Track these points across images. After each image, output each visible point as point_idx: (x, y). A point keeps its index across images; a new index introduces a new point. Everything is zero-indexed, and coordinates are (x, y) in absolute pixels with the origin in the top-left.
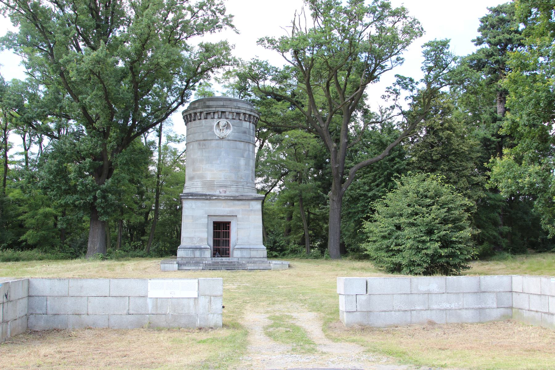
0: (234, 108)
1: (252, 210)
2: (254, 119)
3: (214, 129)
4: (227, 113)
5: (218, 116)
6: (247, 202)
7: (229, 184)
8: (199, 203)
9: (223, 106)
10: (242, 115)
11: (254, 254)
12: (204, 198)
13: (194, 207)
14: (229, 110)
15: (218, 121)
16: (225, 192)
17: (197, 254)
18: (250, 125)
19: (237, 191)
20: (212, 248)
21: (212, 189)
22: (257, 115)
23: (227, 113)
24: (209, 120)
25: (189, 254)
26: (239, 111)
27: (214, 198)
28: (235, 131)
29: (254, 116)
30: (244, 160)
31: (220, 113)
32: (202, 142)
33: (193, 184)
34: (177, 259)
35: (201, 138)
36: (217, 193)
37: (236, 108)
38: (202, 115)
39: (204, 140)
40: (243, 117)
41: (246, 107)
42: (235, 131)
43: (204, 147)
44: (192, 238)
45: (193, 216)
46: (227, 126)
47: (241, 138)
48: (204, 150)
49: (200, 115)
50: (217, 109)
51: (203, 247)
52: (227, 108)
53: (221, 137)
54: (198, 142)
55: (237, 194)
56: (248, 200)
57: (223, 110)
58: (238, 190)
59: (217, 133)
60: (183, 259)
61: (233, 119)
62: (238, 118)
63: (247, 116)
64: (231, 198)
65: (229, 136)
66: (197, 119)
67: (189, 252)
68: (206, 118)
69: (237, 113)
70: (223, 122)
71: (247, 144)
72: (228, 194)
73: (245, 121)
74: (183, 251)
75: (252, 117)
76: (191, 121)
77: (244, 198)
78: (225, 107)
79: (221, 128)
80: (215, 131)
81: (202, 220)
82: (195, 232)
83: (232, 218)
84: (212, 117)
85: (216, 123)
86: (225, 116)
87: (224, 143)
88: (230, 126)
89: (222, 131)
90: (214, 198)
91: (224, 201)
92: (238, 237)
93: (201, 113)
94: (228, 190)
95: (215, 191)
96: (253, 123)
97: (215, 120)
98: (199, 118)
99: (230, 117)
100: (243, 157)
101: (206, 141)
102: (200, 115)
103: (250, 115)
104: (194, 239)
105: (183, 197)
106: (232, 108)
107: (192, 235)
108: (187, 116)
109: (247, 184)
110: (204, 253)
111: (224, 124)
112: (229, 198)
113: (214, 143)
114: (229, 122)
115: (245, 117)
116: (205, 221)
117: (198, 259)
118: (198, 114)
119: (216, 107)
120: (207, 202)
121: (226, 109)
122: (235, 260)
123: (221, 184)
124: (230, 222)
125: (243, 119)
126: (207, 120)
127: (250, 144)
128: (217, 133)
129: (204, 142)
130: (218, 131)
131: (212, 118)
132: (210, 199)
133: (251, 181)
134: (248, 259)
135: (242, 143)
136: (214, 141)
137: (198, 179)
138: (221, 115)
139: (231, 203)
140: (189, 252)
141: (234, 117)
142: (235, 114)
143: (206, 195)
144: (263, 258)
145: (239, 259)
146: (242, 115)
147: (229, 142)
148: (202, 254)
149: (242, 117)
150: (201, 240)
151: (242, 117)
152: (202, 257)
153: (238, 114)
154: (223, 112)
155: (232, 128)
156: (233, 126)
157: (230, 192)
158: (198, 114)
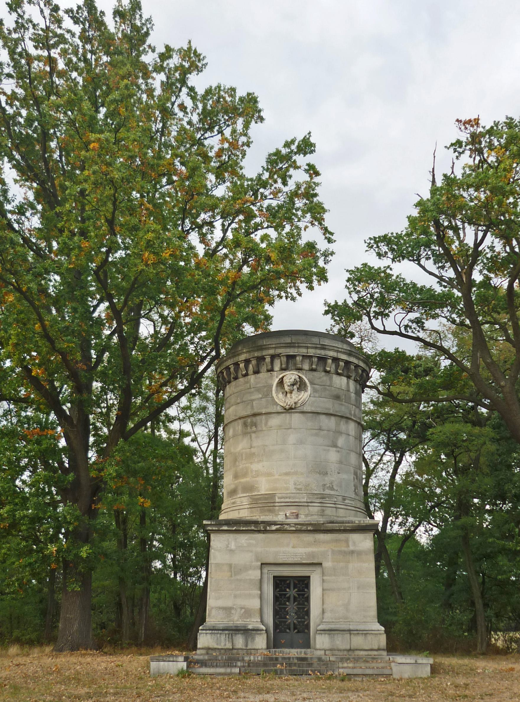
0: (312, 348)
1: (352, 552)
2: (357, 372)
3: (274, 392)
4: (298, 358)
5: (281, 365)
6: (342, 536)
8: (243, 539)
9: (290, 345)
10: (330, 361)
11: (358, 641)
12: (253, 528)
13: (233, 546)
14: (303, 351)
15: (281, 376)
16: (297, 516)
17: (239, 641)
18: (348, 383)
19: (322, 513)
21: (270, 511)
22: (361, 364)
23: (299, 359)
24: (263, 375)
26: (323, 353)
27: (274, 528)
29: (357, 366)
30: (338, 452)
31: (284, 359)
33: (234, 503)
34: (198, 652)
35: (249, 412)
36: (280, 518)
37: (316, 348)
38: (251, 367)
39: (255, 415)
40: (333, 366)
41: (340, 346)
42: (317, 395)
43: (254, 429)
44: (228, 610)
45: (230, 566)
46: (300, 385)
48: (253, 435)
49: (246, 367)
50: (279, 351)
51: (250, 627)
52: (299, 347)
53: (287, 407)
54: (242, 420)
55: (321, 520)
56: (345, 531)
58: (323, 511)
59: (280, 399)
60: (210, 652)
61: (312, 370)
63: (342, 364)
64: (309, 528)
65: (303, 404)
66: (240, 375)
67: (223, 637)
68: (257, 372)
69: (318, 357)
70: (290, 376)
71: (343, 421)
72: (302, 519)
74: (209, 636)
75: (352, 367)
76: (229, 382)
77: (336, 526)
78: (294, 347)
79: (287, 388)
80: (274, 395)
81: (250, 572)
82: (235, 596)
83: (311, 568)
84: (269, 367)
85: (278, 380)
86: (295, 364)
87: (296, 418)
88: (305, 384)
89: (288, 395)
90: (274, 528)
91: (295, 535)
93: (247, 362)
94: (303, 512)
95: (277, 515)
96: (356, 381)
97: (275, 373)
98: (244, 372)
99: (306, 367)
100: (335, 446)
101: (258, 418)
102: (246, 367)
103: (347, 363)
105: (209, 528)
107: (229, 603)
108: (222, 372)
109: (344, 500)
110: (253, 639)
111: (292, 380)
112: (304, 528)
113: (275, 421)
114: (304, 377)
115: (337, 367)
116: (256, 574)
117: (240, 652)
118: (242, 365)
119: (275, 348)
121: (296, 350)
122: (320, 653)
123: (288, 500)
124: (309, 577)
125: (333, 370)
126: (261, 375)
127: (350, 421)
128: (280, 399)
129: (254, 419)
130: (281, 395)
131: (268, 371)
132: (265, 531)
133: (353, 496)
134: (345, 653)
135: (333, 418)
136: (273, 415)
140: (223, 637)
141: (314, 367)
142: (315, 360)
143: (256, 523)
144: (379, 650)
146: (330, 361)
148: (249, 642)
149: (330, 366)
150: (248, 612)
151: (330, 366)
152: (249, 647)
153: (322, 360)
154: (291, 358)
155: (309, 388)
156: (312, 383)
157: (306, 515)
158: (242, 365)
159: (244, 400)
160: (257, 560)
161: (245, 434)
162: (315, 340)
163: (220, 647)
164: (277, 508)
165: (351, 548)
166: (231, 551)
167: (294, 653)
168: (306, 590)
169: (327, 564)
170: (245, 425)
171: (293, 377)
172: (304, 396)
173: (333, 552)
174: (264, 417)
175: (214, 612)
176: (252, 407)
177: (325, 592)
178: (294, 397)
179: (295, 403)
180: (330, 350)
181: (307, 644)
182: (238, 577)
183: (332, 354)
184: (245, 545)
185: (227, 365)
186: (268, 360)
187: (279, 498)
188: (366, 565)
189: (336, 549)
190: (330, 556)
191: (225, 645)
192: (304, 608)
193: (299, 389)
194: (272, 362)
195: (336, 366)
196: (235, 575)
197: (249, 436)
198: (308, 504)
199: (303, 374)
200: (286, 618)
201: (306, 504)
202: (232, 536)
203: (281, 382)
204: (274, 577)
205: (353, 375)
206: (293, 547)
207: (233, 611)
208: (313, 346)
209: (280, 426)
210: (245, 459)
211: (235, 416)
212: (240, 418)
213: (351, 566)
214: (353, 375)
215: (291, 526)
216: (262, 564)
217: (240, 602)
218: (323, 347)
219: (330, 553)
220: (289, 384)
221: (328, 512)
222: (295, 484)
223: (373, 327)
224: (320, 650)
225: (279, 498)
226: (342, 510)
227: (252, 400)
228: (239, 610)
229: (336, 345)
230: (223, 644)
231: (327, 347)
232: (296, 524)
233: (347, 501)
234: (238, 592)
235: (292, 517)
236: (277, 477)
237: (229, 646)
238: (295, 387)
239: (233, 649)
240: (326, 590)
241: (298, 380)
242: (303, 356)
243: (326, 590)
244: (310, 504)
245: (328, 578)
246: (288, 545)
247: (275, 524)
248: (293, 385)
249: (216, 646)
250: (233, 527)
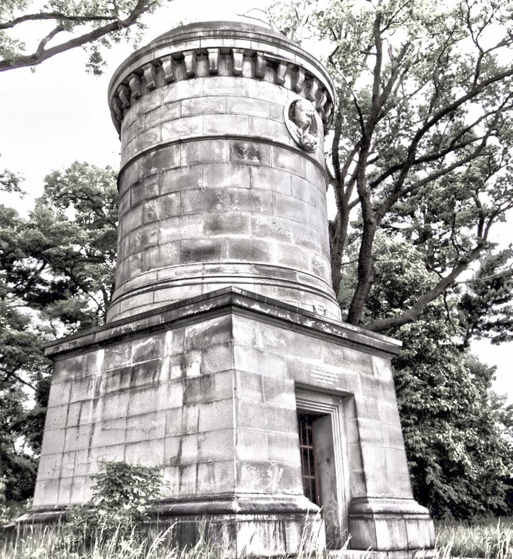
12: (288, 317)
32: (246, 145)
39: (258, 140)
43: (256, 160)
45: (259, 378)
104: (270, 473)
123: (311, 285)
129: (256, 146)
137: (237, 257)
159: (234, 110)
161: (238, 164)
164: (302, 293)
165: (376, 377)
170: (238, 150)
174: (272, 148)
176: (251, 127)
182: (271, 403)
185: (203, 46)
187: (301, 278)
196: (267, 399)
197: (246, 168)
209: (295, 171)
210: (239, 204)
211: (212, 131)
212: (227, 137)
215: (327, 327)
219: (359, 380)
225: (301, 278)
227: (252, 117)
228: (276, 469)
236: (293, 244)
250: (266, 309)
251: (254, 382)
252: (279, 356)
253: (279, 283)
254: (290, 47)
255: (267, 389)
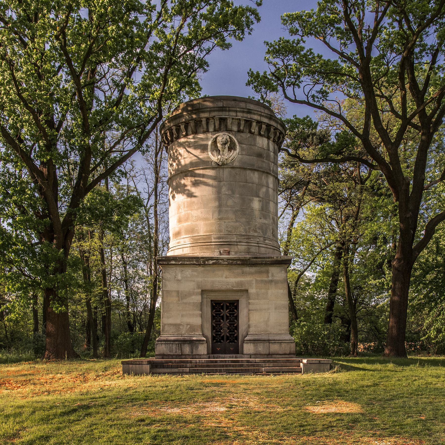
1: (272, 281)
4: (228, 121)
5: (215, 126)
7: (235, 240)
8: (188, 272)
10: (254, 124)
13: (180, 278)
15: (215, 136)
16: (229, 253)
17: (187, 349)
20: (210, 340)
23: (229, 122)
25: (175, 349)
28: (244, 153)
37: (243, 112)
41: (263, 111)
42: (244, 153)
44: (177, 326)
45: (178, 292)
47: (253, 165)
52: (229, 111)
53: (220, 163)
57: (224, 115)
58: (249, 249)
61: (239, 131)
62: (248, 131)
63: (264, 126)
65: (233, 161)
67: (174, 346)
69: (245, 120)
73: (260, 134)
74: (163, 346)
81: (193, 297)
82: (182, 316)
83: (239, 294)
86: (226, 126)
92: (250, 322)
94: (234, 249)
99: (235, 128)
104: (181, 327)
106: (236, 111)
107: (178, 321)
111: (224, 140)
114: (234, 138)
115: (260, 129)
116: (198, 299)
120: (200, 269)
124: (238, 301)
125: (256, 132)
132: (204, 265)
138: (220, 124)
139: (238, 270)
140: (174, 346)
142: (243, 123)
145: (252, 356)
146: (254, 124)
147: (233, 171)
148: (194, 350)
149: (255, 128)
150: (192, 328)
151: (255, 128)
153: (249, 123)
155: (238, 147)
156: (240, 143)
157: (236, 253)
160: (198, 288)
162: (243, 105)
163: (172, 354)
165: (270, 278)
166: (179, 281)
167: (228, 358)
168: (235, 311)
169: (252, 291)
171: (225, 137)
172: (234, 154)
173: (256, 281)
175: (166, 328)
177: (250, 312)
178: (226, 155)
179: (226, 159)
180: (254, 114)
181: (237, 351)
182: (185, 301)
183: (256, 117)
184: (189, 276)
186: (204, 123)
188: (281, 291)
189: (259, 279)
190: (254, 285)
191: (176, 352)
192: (234, 324)
193: (230, 149)
194: (207, 124)
195: (259, 128)
196: (182, 299)
198: (237, 243)
199: (233, 135)
200: (220, 332)
201: (236, 243)
202: (178, 269)
203: (215, 142)
204: (212, 301)
205: (272, 136)
206: (226, 278)
207: (181, 327)
208: (241, 110)
213: (270, 292)
214: (272, 136)
216: (202, 291)
217: (186, 320)
218: (249, 112)
219: (254, 282)
220: (221, 143)
221: (253, 249)
222: (227, 227)
223: (286, 97)
224: (247, 355)
226: (263, 249)
228: (185, 326)
229: (260, 110)
230: (174, 351)
231: (252, 111)
232: (228, 260)
233: (267, 242)
234: (184, 313)
235: (225, 254)
237: (179, 352)
238: (227, 146)
239: (182, 355)
240: (252, 310)
241: (229, 140)
242: (233, 119)
243: (252, 310)
244: (239, 244)
245: (253, 301)
246: (222, 276)
247: (212, 259)
248: (224, 144)
249: (169, 353)
251: (175, 294)
252: (191, 281)
253: (200, 244)
254: (205, 110)
255: (181, 295)
